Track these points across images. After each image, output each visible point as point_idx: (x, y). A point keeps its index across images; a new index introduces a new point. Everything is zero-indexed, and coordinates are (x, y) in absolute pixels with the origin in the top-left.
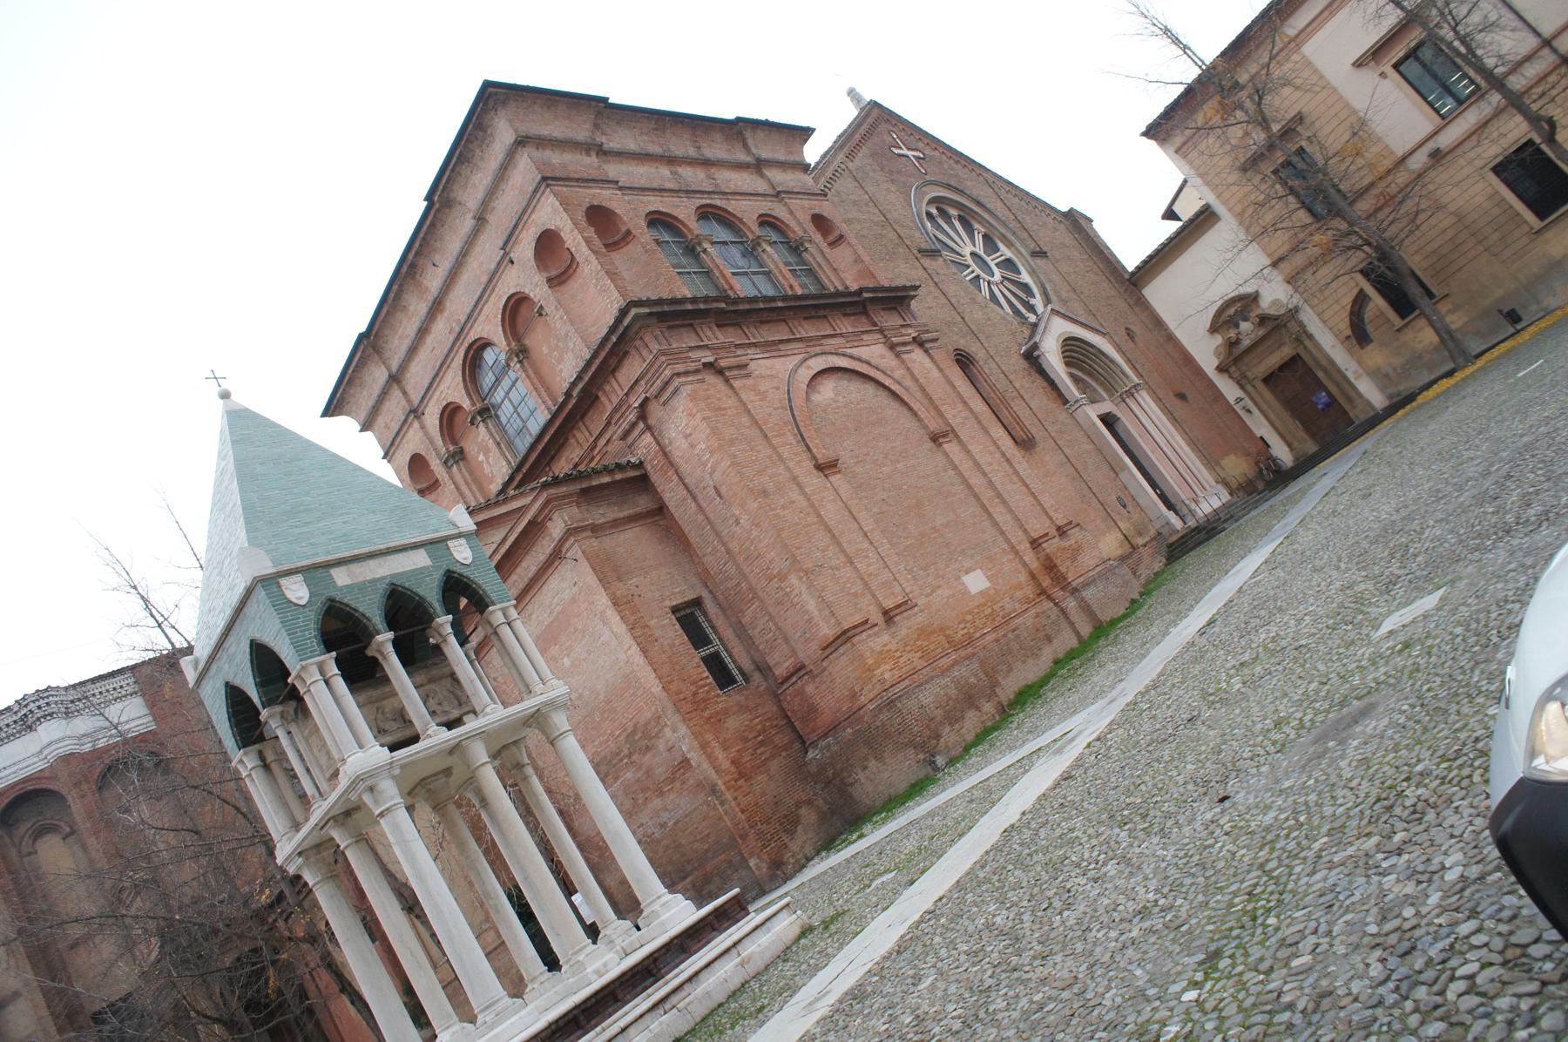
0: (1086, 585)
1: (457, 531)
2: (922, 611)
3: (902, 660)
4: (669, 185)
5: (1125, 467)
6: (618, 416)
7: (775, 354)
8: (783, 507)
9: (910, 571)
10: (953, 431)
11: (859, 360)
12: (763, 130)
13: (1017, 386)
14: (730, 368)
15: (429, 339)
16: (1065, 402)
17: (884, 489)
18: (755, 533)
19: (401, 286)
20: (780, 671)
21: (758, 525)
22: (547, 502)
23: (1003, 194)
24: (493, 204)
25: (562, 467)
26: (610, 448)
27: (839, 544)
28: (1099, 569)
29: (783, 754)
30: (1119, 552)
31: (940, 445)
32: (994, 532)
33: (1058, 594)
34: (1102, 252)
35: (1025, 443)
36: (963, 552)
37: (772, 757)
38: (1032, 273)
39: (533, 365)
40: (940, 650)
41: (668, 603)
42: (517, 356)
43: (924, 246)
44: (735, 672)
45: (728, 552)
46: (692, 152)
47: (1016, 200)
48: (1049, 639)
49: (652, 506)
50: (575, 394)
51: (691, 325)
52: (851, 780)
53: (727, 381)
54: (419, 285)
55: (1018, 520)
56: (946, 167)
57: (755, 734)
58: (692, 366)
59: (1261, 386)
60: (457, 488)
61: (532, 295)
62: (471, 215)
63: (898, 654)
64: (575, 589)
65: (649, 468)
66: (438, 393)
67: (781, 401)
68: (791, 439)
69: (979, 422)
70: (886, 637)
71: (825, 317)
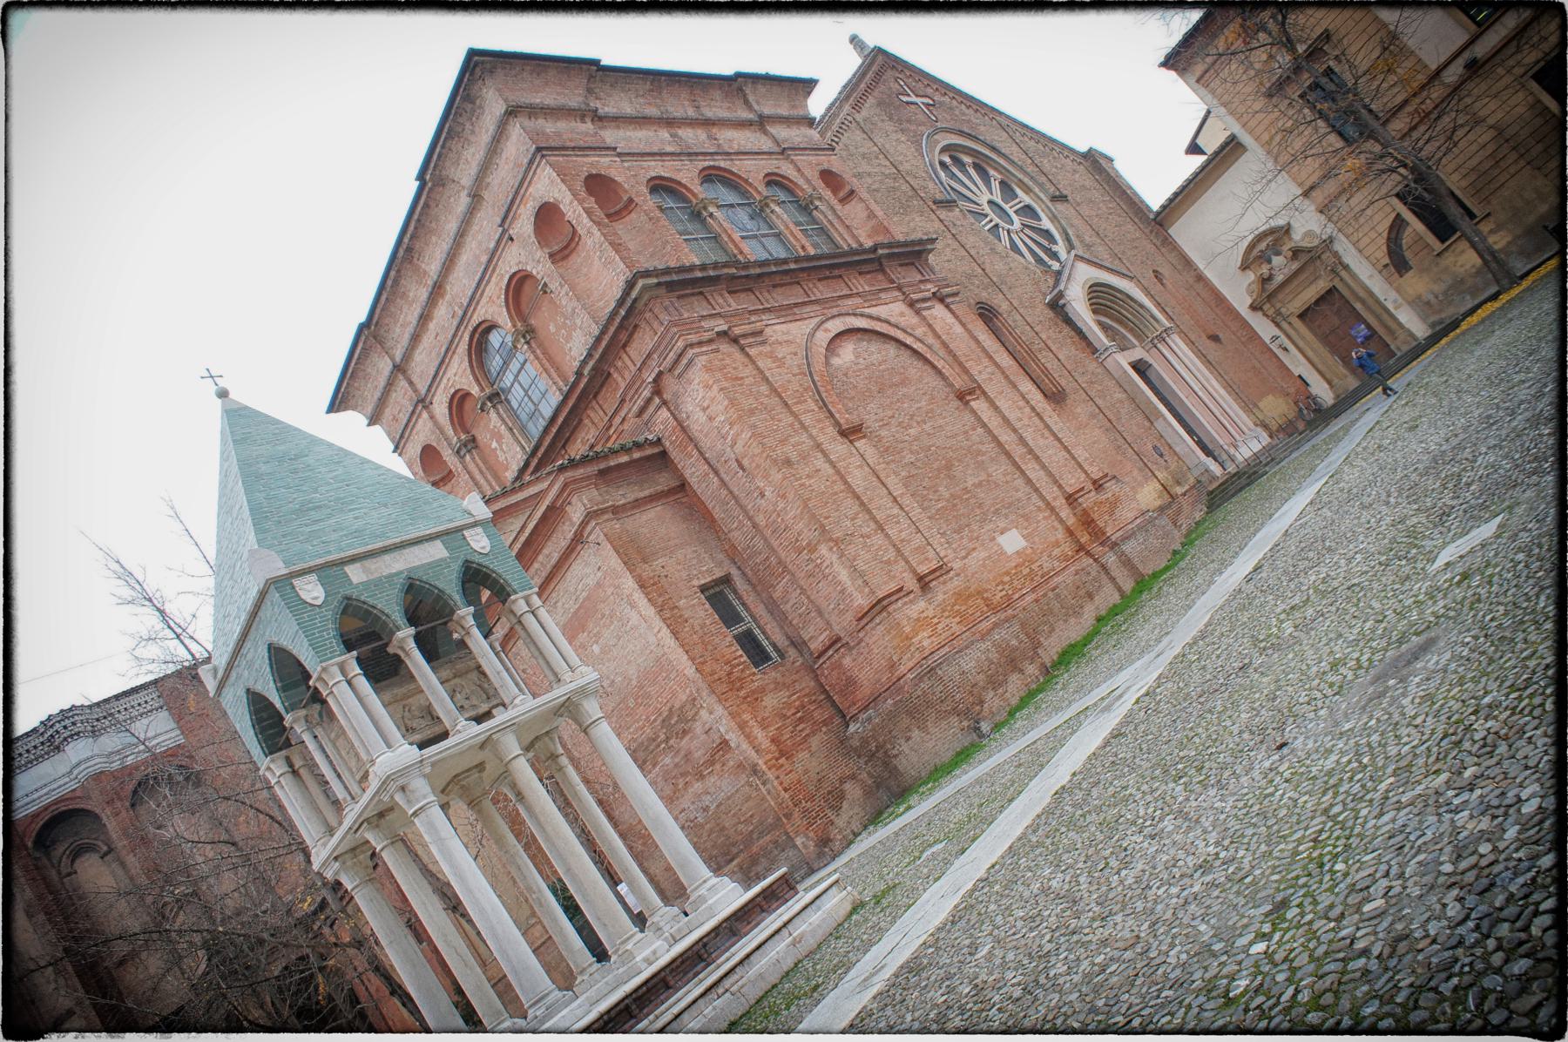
0: (1126, 538)
1: (472, 520)
2: (958, 575)
3: (940, 626)
4: (669, 149)
5: (1160, 415)
6: (632, 392)
7: (790, 318)
8: (808, 476)
9: (943, 534)
10: (979, 387)
11: (879, 319)
12: (764, 85)
13: (1044, 336)
14: (744, 336)
15: (432, 326)
16: (1095, 350)
17: (912, 452)
18: (781, 505)
19: (398, 271)
20: (815, 646)
21: (784, 496)
22: (566, 485)
23: (1018, 137)
24: (488, 180)
25: (578, 449)
26: (626, 426)
27: (869, 511)
28: (1138, 521)
29: (824, 729)
30: (1158, 503)
31: (967, 403)
32: (1028, 489)
33: (1097, 549)
34: (1124, 192)
35: (1056, 397)
36: (997, 512)
37: (813, 733)
38: (1054, 218)
39: (540, 345)
40: (979, 614)
41: (696, 583)
42: (524, 337)
43: (938, 197)
44: (770, 649)
45: (755, 526)
46: (691, 113)
47: (1032, 143)
48: (1090, 596)
49: (674, 483)
50: (586, 372)
51: (701, 293)
52: (895, 752)
53: (742, 349)
54: (417, 269)
55: (1050, 474)
56: (957, 112)
57: (793, 711)
58: (706, 336)
59: (1298, 323)
60: (472, 478)
61: (534, 272)
62: (466, 192)
63: (936, 620)
64: (599, 574)
65: (667, 444)
66: (445, 381)
69: (1007, 377)
70: (922, 604)
71: (840, 276)
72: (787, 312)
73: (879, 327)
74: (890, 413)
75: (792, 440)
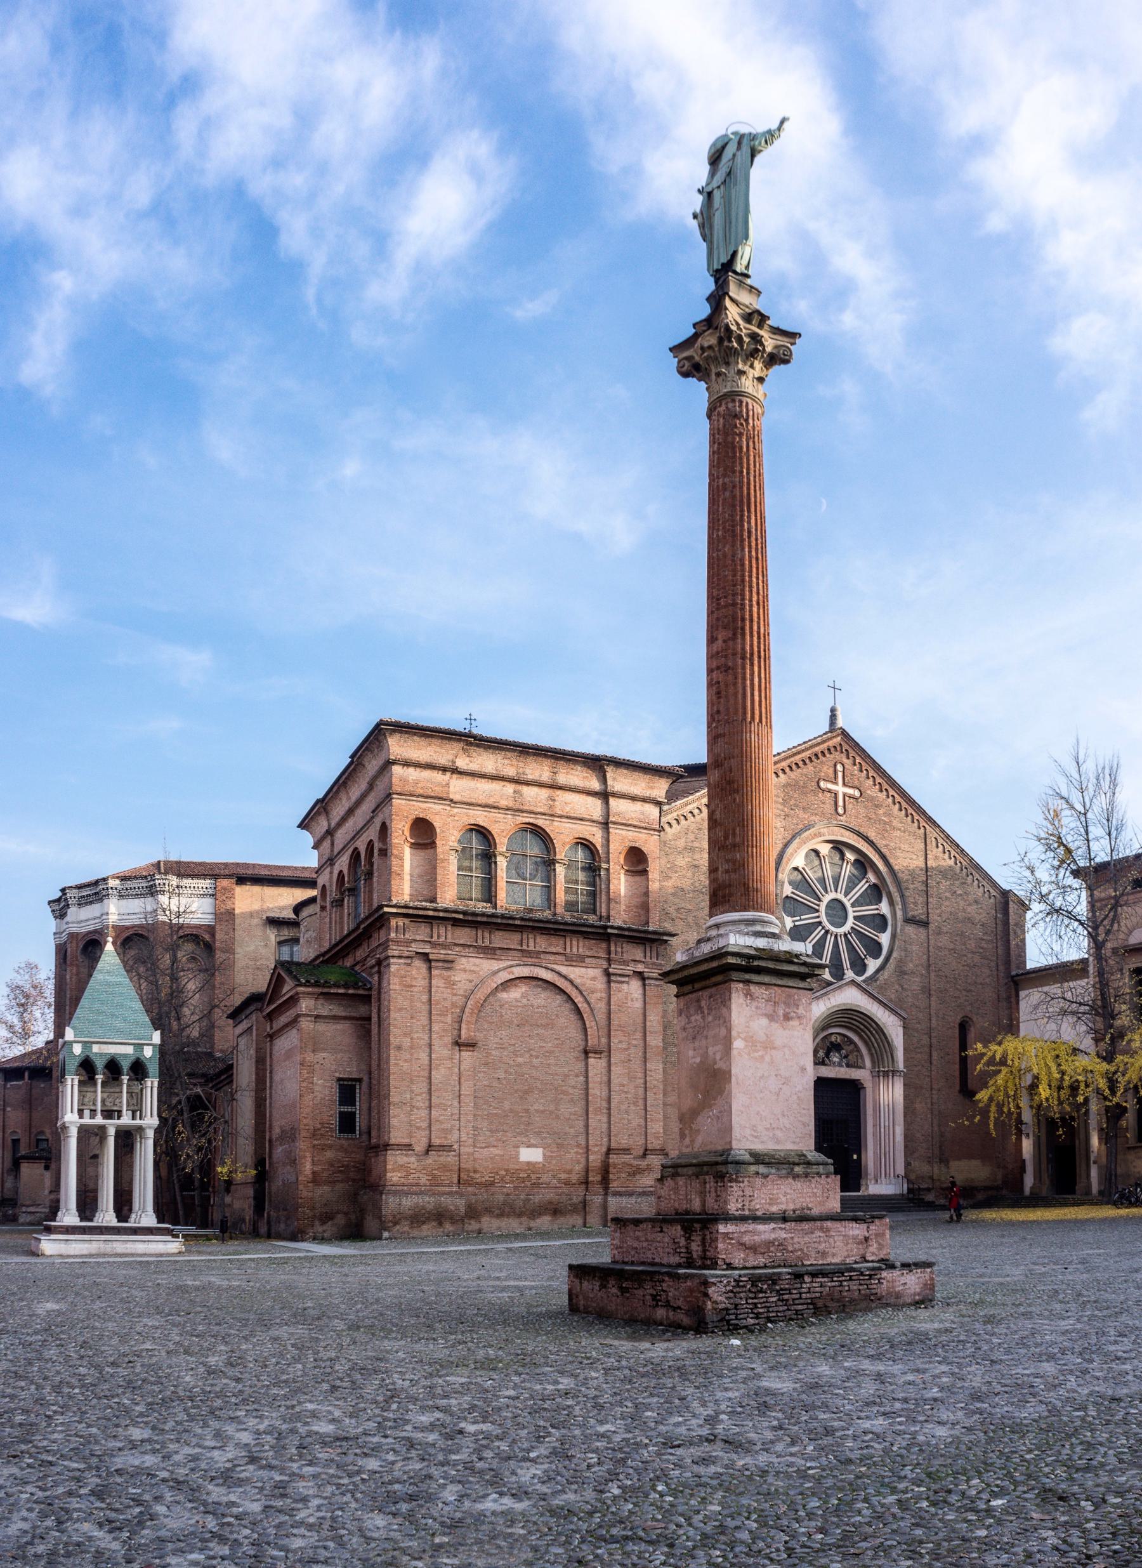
4: (503, 803)
8: (406, 1061)
10: (609, 1051)
11: (565, 977)
36: (539, 1133)
55: (609, 1128)
58: (406, 954)
67: (466, 991)
68: (449, 1019)
70: (413, 1159)
72: (489, 952)
73: (560, 982)
74: (513, 1042)
75: (415, 1036)
